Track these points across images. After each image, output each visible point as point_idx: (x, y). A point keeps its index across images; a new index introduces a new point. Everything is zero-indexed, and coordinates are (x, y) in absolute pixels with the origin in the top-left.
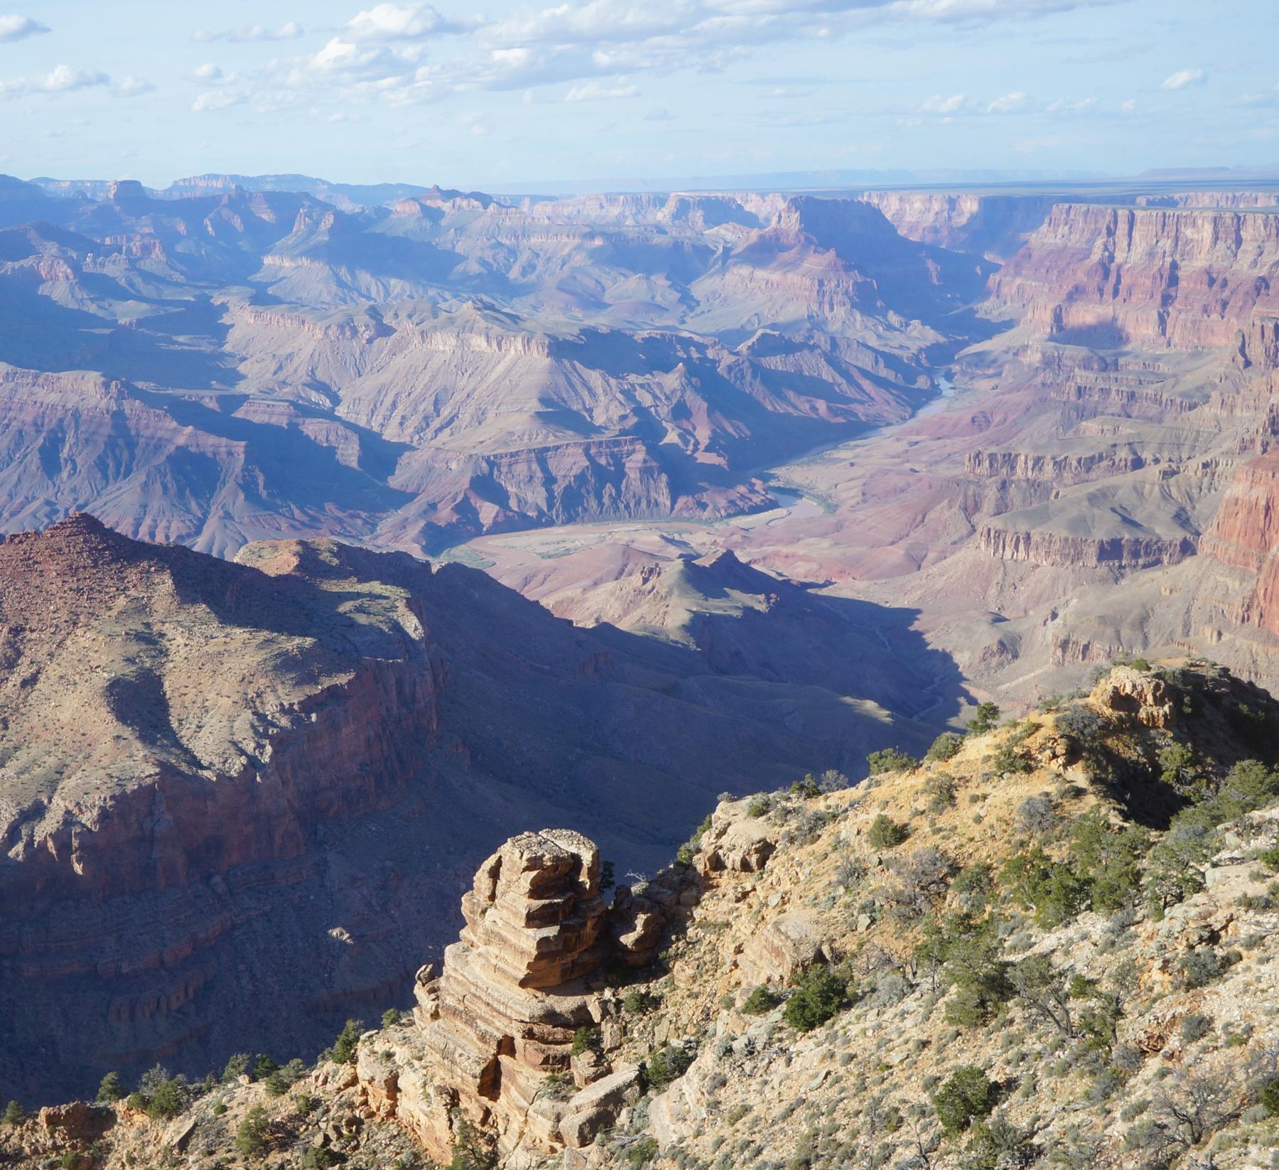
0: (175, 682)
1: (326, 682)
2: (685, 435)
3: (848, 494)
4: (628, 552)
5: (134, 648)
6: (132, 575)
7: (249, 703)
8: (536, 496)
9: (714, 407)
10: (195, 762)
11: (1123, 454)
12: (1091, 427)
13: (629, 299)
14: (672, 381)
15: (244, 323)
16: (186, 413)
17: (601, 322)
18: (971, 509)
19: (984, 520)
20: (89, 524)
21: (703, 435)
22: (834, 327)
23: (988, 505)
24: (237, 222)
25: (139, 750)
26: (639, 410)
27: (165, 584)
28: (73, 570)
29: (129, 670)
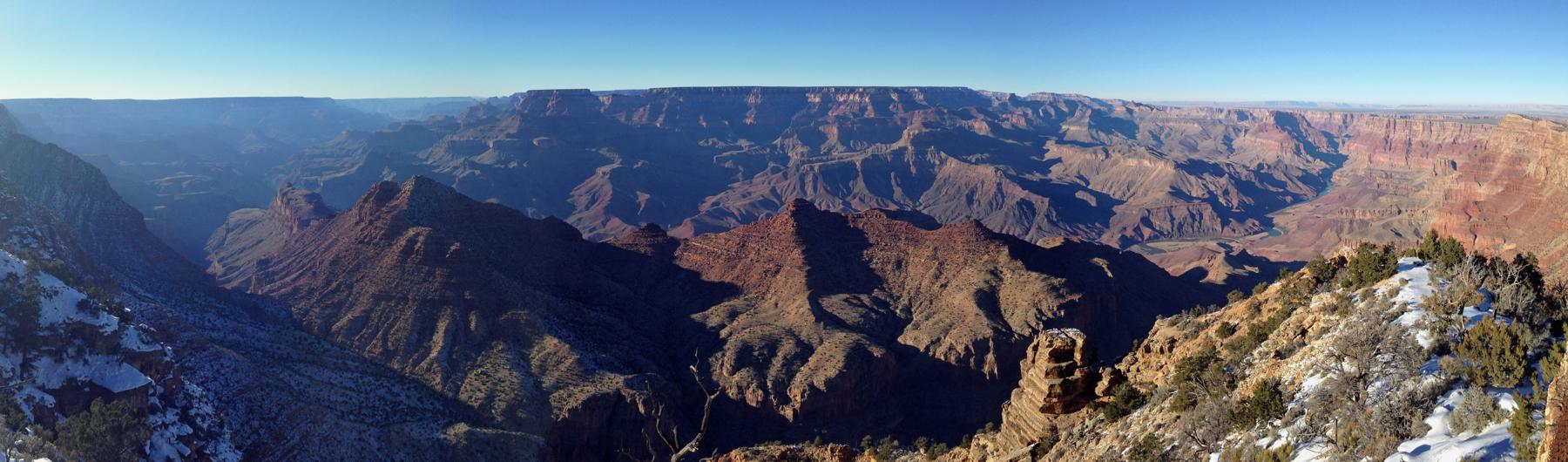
0: (1004, 294)
1: (1069, 298)
2: (1228, 201)
3: (1293, 227)
4: (1203, 249)
5: (989, 277)
6: (992, 247)
7: (1035, 305)
8: (1167, 226)
9: (1239, 190)
10: (1009, 328)
11: (1395, 209)
12: (1383, 199)
13: (1207, 150)
14: (1223, 181)
15: (1053, 150)
16: (1026, 184)
17: (1195, 157)
18: (1339, 231)
19: (1344, 236)
20: (978, 223)
21: (1235, 203)
22: (1287, 162)
23: (1346, 230)
24: (1052, 112)
25: (985, 321)
26: (1210, 192)
27: (1005, 251)
28: (968, 242)
29: (985, 287)
